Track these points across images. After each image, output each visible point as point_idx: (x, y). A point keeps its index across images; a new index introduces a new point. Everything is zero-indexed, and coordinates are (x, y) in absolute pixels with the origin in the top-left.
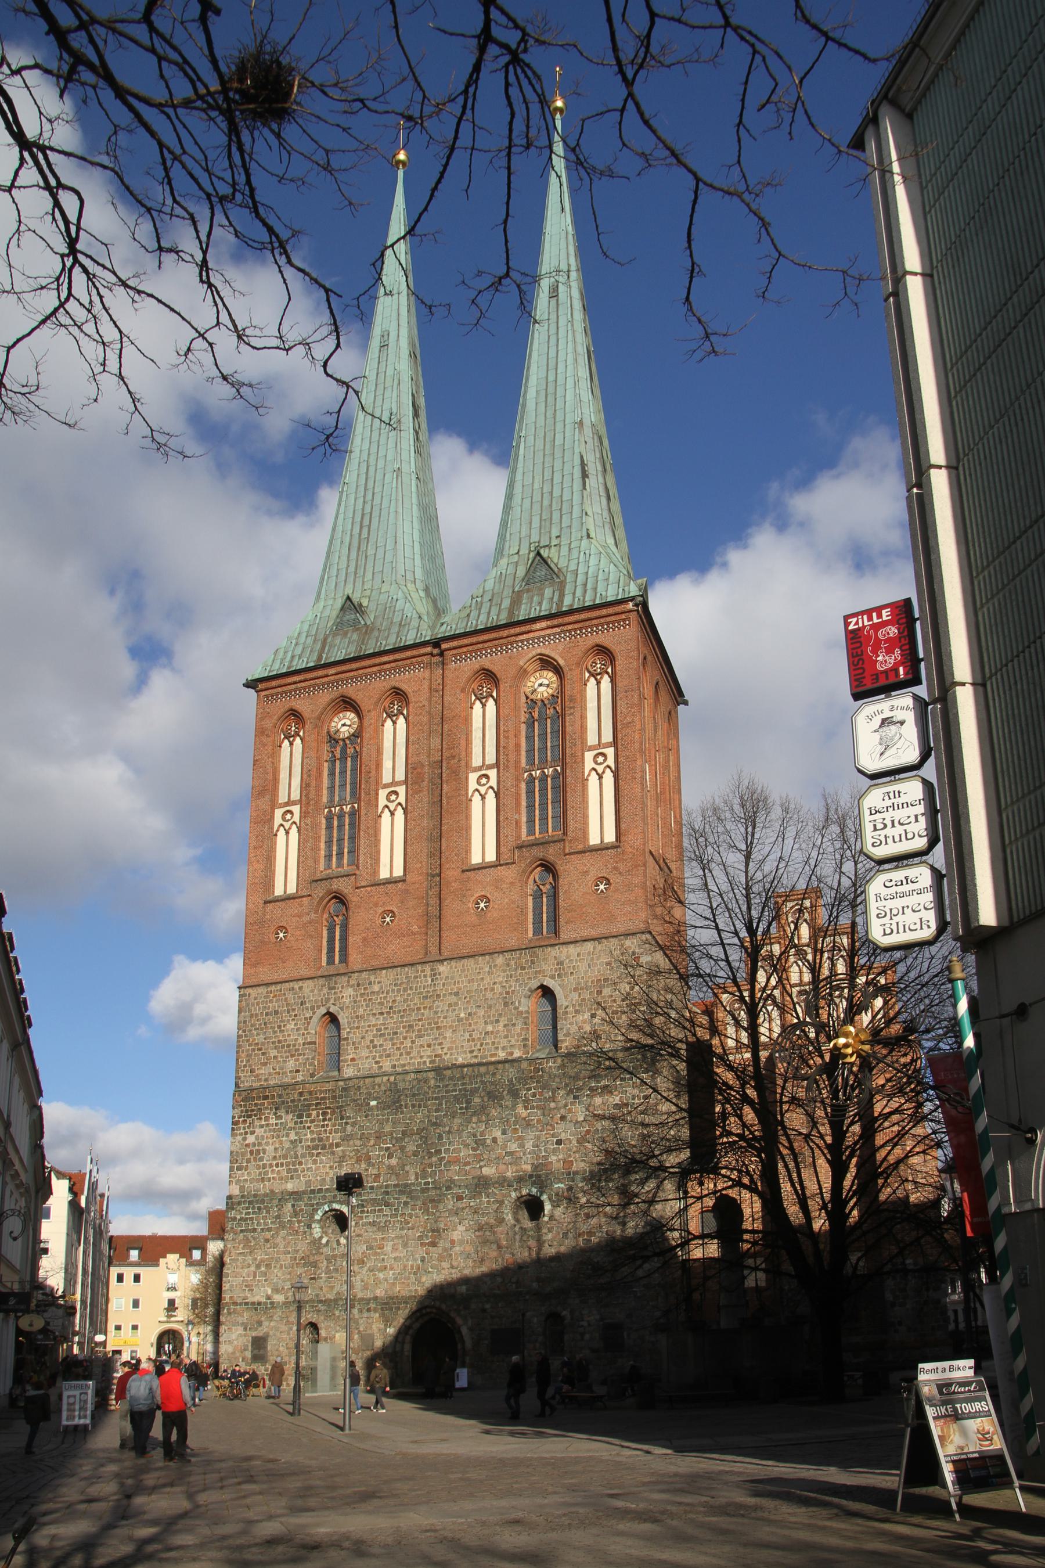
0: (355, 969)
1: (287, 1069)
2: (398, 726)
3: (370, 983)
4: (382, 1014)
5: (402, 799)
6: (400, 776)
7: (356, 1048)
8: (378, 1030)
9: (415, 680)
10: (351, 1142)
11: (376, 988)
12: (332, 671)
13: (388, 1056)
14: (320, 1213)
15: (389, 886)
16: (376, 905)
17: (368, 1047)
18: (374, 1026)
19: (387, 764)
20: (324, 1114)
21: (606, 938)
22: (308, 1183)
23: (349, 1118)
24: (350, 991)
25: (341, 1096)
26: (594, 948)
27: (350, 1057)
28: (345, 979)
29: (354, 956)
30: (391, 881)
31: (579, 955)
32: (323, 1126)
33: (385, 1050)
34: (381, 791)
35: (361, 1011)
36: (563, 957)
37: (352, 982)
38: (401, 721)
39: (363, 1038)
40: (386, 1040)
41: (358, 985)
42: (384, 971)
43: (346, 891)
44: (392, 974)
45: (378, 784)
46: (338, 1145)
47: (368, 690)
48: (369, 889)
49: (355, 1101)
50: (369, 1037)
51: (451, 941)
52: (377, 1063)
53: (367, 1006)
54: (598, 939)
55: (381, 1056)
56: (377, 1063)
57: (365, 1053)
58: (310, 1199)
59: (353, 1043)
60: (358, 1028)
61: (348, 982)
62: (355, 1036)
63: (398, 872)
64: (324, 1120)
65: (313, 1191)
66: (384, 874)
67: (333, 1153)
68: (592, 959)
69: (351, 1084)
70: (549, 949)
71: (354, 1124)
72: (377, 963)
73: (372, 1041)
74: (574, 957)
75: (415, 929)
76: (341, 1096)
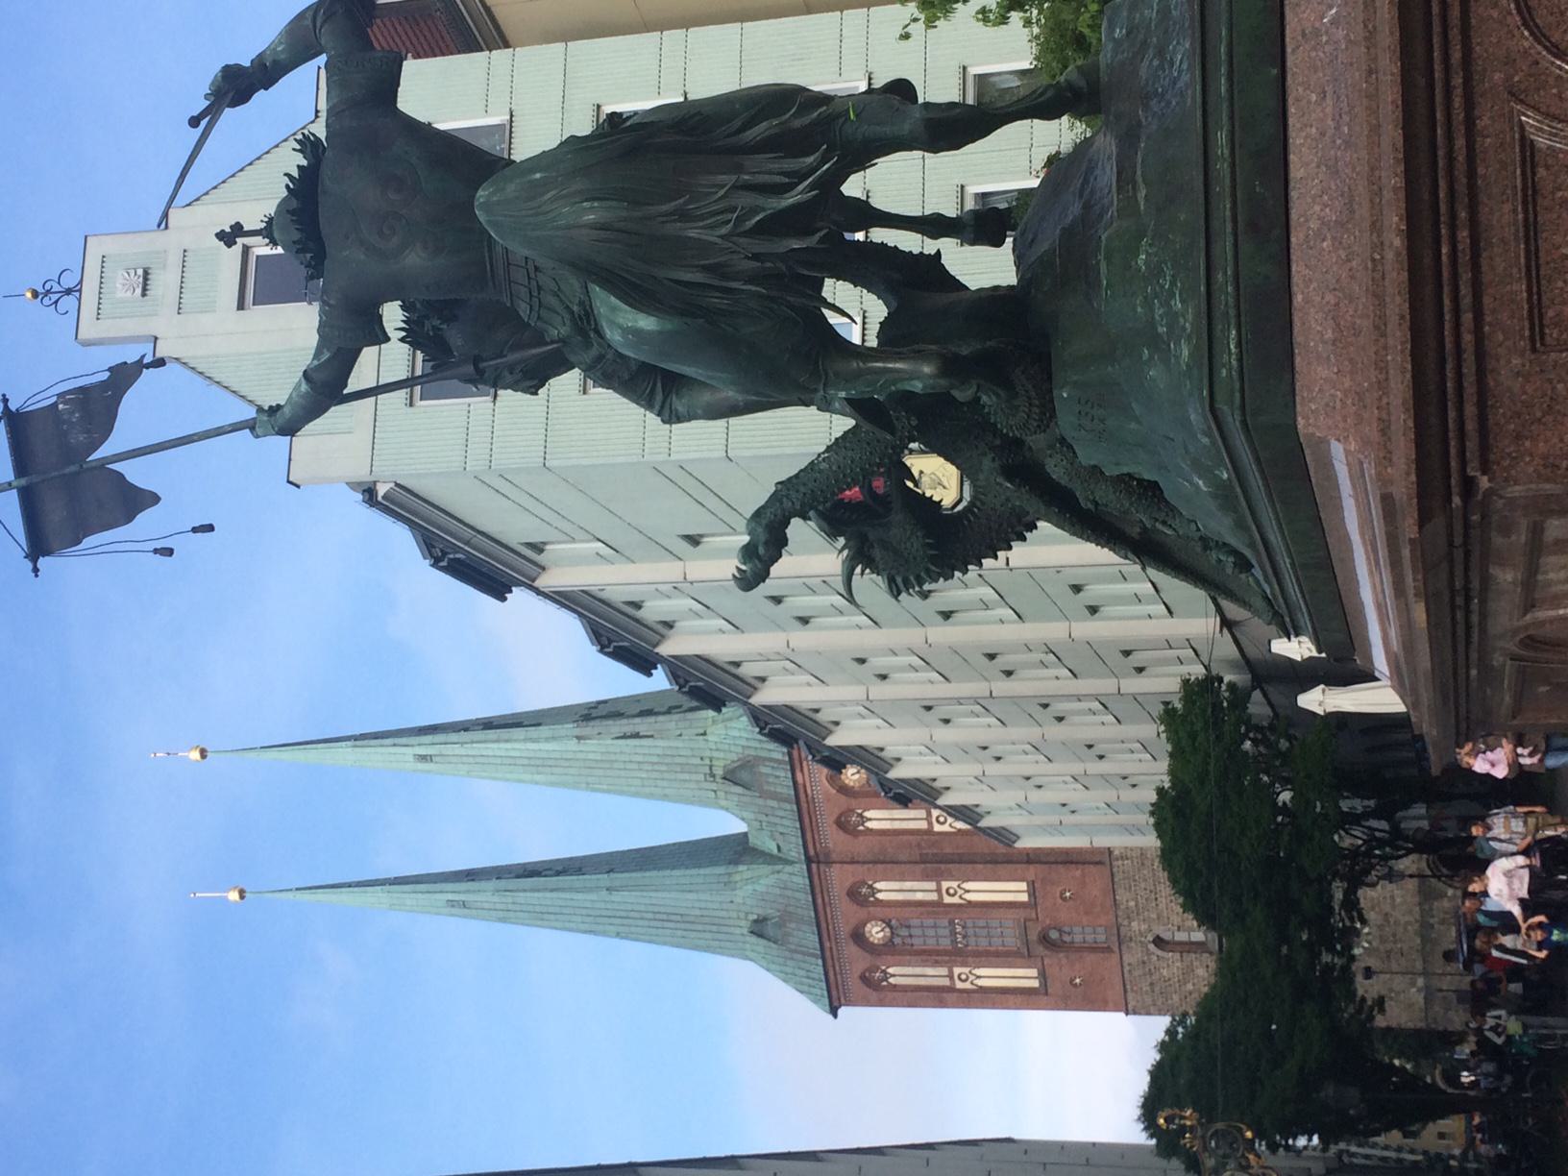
5: (954, 884)
6: (932, 885)
9: (839, 878)
12: (827, 945)
19: (919, 896)
30: (1032, 891)
38: (878, 886)
45: (939, 904)
63: (1023, 886)
66: (1024, 897)
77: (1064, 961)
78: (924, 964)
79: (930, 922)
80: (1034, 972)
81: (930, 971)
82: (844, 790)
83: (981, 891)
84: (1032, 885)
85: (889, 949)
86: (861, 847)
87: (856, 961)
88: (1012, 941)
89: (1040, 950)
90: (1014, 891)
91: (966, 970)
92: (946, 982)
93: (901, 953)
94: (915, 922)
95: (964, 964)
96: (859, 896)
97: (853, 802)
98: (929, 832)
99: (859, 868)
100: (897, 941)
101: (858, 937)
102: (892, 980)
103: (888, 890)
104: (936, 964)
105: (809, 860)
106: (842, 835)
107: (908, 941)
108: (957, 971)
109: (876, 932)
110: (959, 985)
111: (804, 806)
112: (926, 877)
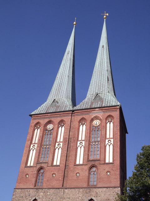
0: (44, 188)
3: (47, 192)
5: (61, 146)
6: (62, 140)
11: (49, 194)
12: (49, 115)
16: (52, 171)
24: (42, 194)
28: (41, 190)
29: (44, 184)
30: (56, 166)
34: (56, 143)
37: (43, 191)
41: (44, 192)
44: (53, 190)
45: (56, 141)
47: (57, 120)
53: (46, 198)
63: (58, 164)
70: (94, 189)
72: (50, 187)
74: (101, 192)
77: (34, 173)
78: (40, 137)
80: (32, 165)
81: (37, 139)
82: (92, 120)
85: (45, 129)
86: (75, 123)
87: (43, 122)
88: (41, 160)
90: (57, 161)
91: (36, 147)
92: (33, 142)
93: (43, 132)
94: (51, 136)
95: (38, 147)
96: (61, 123)
97: (88, 122)
99: (69, 123)
100: (47, 131)
101: (50, 122)
102: (36, 129)
103: (62, 131)
104: (39, 140)
105: (73, 111)
106: (79, 119)
107: (47, 134)
108: (36, 145)
109: (50, 127)
110: (32, 145)
111: (89, 110)
112: (64, 139)
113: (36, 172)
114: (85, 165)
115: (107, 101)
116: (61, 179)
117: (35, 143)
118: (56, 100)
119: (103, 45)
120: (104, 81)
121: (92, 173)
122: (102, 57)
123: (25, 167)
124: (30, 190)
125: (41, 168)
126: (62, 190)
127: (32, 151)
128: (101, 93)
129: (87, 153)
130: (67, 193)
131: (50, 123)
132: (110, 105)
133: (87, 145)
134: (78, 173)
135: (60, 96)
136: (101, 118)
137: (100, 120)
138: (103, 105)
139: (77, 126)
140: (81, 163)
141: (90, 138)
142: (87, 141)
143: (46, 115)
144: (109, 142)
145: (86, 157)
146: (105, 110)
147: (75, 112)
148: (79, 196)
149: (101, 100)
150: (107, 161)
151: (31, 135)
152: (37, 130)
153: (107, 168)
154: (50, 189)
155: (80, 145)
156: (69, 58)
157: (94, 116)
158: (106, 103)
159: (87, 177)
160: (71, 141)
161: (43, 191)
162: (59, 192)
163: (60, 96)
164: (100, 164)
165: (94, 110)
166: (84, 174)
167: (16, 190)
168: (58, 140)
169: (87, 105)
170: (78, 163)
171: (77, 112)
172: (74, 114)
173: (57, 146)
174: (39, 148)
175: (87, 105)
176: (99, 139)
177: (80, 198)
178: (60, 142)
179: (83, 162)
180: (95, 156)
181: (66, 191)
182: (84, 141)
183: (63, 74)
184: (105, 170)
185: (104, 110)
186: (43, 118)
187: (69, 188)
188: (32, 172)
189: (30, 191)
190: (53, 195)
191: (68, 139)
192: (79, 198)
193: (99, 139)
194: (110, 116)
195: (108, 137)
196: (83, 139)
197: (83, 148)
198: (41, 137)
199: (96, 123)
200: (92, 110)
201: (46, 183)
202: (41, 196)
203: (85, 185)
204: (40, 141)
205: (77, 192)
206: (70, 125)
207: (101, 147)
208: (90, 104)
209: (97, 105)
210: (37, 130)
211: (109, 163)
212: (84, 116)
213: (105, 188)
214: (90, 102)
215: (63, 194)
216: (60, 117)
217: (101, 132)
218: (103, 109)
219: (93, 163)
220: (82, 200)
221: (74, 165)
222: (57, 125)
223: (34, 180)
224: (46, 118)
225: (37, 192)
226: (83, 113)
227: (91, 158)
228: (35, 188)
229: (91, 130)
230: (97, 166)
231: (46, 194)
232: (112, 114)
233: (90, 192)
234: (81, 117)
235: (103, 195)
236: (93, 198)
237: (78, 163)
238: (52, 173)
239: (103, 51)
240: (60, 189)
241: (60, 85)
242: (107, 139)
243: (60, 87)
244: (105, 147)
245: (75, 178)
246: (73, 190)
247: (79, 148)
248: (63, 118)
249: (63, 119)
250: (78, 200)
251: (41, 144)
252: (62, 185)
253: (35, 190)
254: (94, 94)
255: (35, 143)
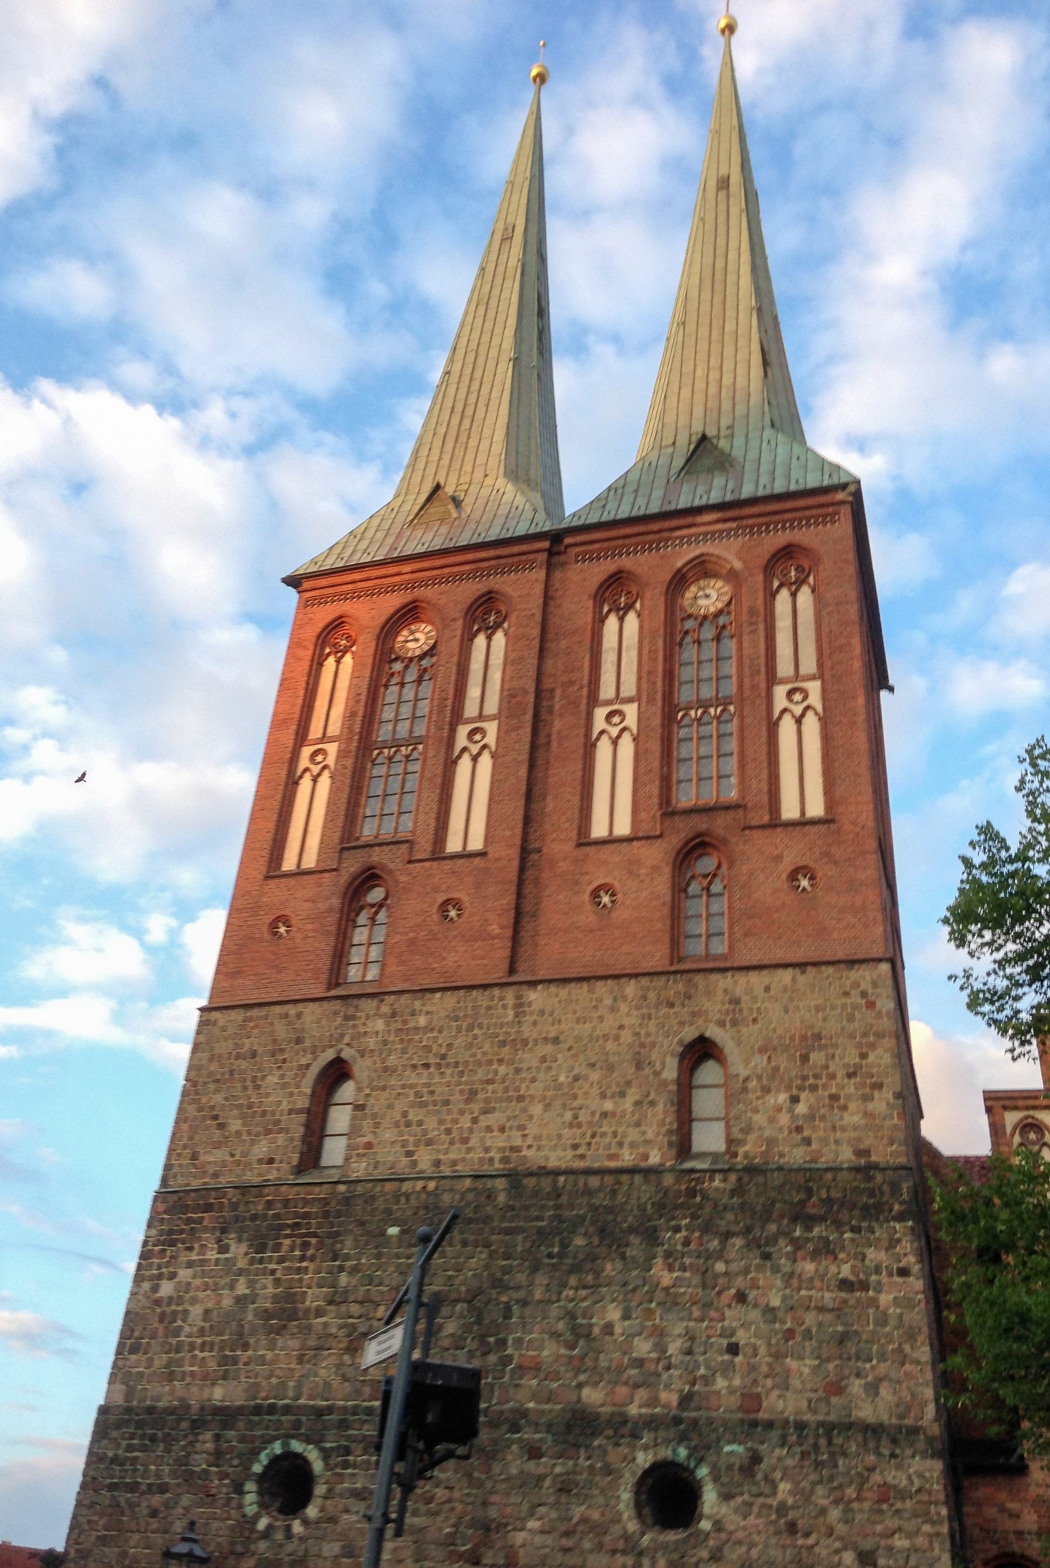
1: (262, 1156)
2: (493, 643)
3: (413, 1014)
4: (427, 1066)
5: (491, 739)
6: (492, 706)
7: (377, 1125)
8: (417, 1095)
10: (343, 1308)
11: (422, 1021)
12: (407, 568)
13: (429, 1143)
14: (264, 1458)
15: (460, 862)
16: (436, 889)
17: (397, 1125)
18: (411, 1086)
19: (473, 692)
20: (305, 1245)
21: (815, 964)
22: (253, 1390)
23: (347, 1257)
24: (380, 1025)
25: (339, 1214)
26: (794, 980)
27: (365, 1140)
29: (392, 968)
30: (465, 855)
31: (767, 989)
32: (299, 1270)
33: (425, 1132)
35: (393, 1060)
36: (738, 992)
37: (385, 1009)
39: (390, 1107)
40: (428, 1113)
41: (394, 1015)
42: (438, 995)
43: (392, 866)
44: (450, 1000)
46: (319, 1313)
48: (427, 864)
49: (362, 1224)
50: (400, 1105)
51: (548, 952)
52: (409, 1154)
53: (404, 1051)
54: (801, 966)
55: (417, 1144)
56: (409, 1154)
57: (389, 1135)
58: (252, 1425)
59: (374, 1116)
60: (384, 1088)
61: (378, 1008)
62: (377, 1103)
63: (476, 843)
64: (302, 1259)
65: (258, 1410)
67: (309, 1328)
68: (791, 1000)
69: (359, 1189)
70: (714, 977)
71: (355, 1270)
72: (427, 982)
73: (405, 1114)
74: (759, 991)
75: (495, 929)
76: (339, 1214)
77: (322, 906)
79: (424, 707)
82: (679, 581)
83: (475, 784)
84: (482, 854)
89: (352, 865)
91: (331, 760)
92: (315, 730)
94: (426, 689)
95: (341, 755)
97: (654, 598)
98: (593, 700)
99: (535, 605)
100: (398, 666)
102: (331, 661)
103: (491, 655)
104: (350, 715)
108: (332, 749)
109: (416, 639)
111: (655, 526)
112: (509, 696)
113: (336, 902)
114: (647, 838)
115: (765, 467)
116: (498, 926)
117: (324, 738)
118: (449, 490)
119: (723, 172)
120: (741, 370)
121: (694, 888)
122: (721, 241)
123: (268, 877)
124: (300, 1007)
125: (370, 877)
126: (510, 995)
127: (306, 783)
128: (723, 432)
129: (656, 764)
130: (542, 1013)
131: (417, 619)
132: (793, 487)
133: (657, 721)
134: (607, 888)
135: (468, 467)
136: (738, 565)
137: (732, 576)
138: (747, 491)
139: (586, 618)
140: (623, 827)
141: (671, 686)
142: (651, 700)
143: (391, 570)
144: (798, 697)
145: (654, 789)
146: (761, 520)
147: (568, 540)
148: (621, 1027)
149: (724, 463)
150: (790, 810)
151: (302, 693)
152: (338, 662)
153: (793, 851)
154: (428, 995)
155: (609, 728)
156: (513, 262)
157: (691, 555)
158: (764, 479)
159: (666, 910)
160: (551, 711)
161: (385, 1009)
162: (489, 1008)
163: (468, 467)
164: (744, 829)
165: (689, 520)
166: (645, 894)
167: (216, 1015)
168: (471, 709)
169: (641, 502)
170: (599, 830)
171: (579, 538)
172: (563, 558)
173: (461, 741)
174: (349, 762)
175: (641, 502)
176: (730, 688)
177: (626, 1036)
178: (481, 717)
179: (635, 822)
180: (709, 778)
181: (535, 996)
182: (635, 705)
183: (483, 350)
184: (778, 859)
185: (750, 522)
186: (370, 593)
187: (550, 981)
188: (314, 902)
189: (299, 1015)
190: (450, 1027)
191: (531, 698)
192: (617, 1038)
193: (730, 688)
194: (787, 552)
195: (784, 667)
196: (629, 688)
197: (627, 747)
198: (363, 698)
199: (709, 597)
200: (674, 523)
201: (402, 963)
202: (372, 1042)
203: (657, 957)
204: (359, 719)
205: (608, 1002)
206: (538, 618)
207: (742, 729)
208: (658, 493)
209: (708, 492)
210: (338, 662)
211: (803, 823)
212: (626, 562)
213: (786, 966)
214: (660, 483)
215: (517, 1015)
216: (471, 576)
217: (740, 643)
218: (746, 511)
219: (700, 823)
220: (642, 1045)
221: (580, 845)
222: (460, 623)
223: (325, 946)
224: (391, 589)
225: (347, 1018)
226: (620, 542)
227: (686, 797)
228: (333, 993)
229: (673, 635)
230: (725, 841)
231: (405, 1022)
232: (803, 536)
233: (689, 997)
234: (608, 566)
235: (775, 1011)
236: (714, 1032)
237: (599, 830)
238: (441, 898)
239: (722, 207)
240: (496, 992)
241: (469, 412)
242: (784, 681)
243: (467, 423)
244: (773, 727)
245: (588, 917)
246: (581, 991)
247: (604, 749)
248: (495, 582)
249: (496, 587)
250: (610, 1046)
251: (364, 744)
252: (505, 966)
253: (336, 1005)
254: (683, 440)
255: (324, 738)
